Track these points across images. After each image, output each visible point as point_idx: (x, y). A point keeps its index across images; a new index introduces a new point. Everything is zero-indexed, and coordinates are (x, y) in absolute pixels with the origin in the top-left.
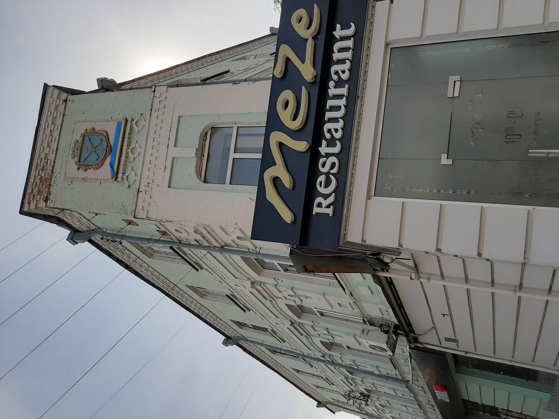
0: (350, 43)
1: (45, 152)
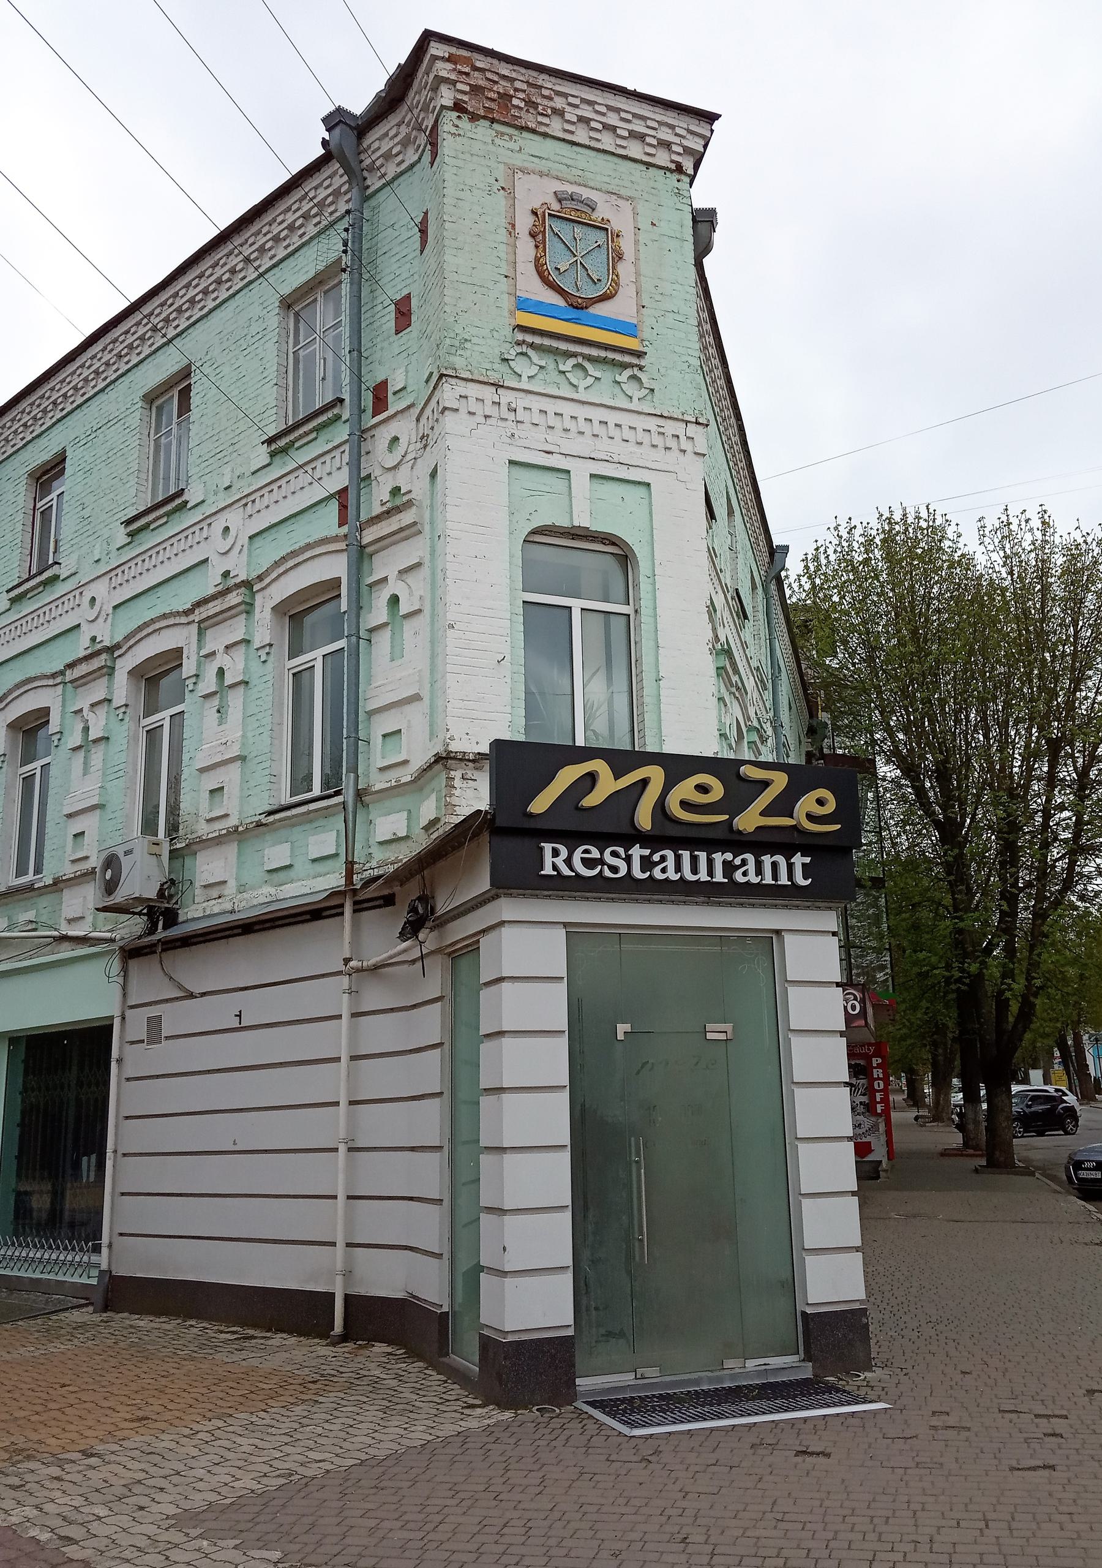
0: (784, 880)
1: (568, 109)
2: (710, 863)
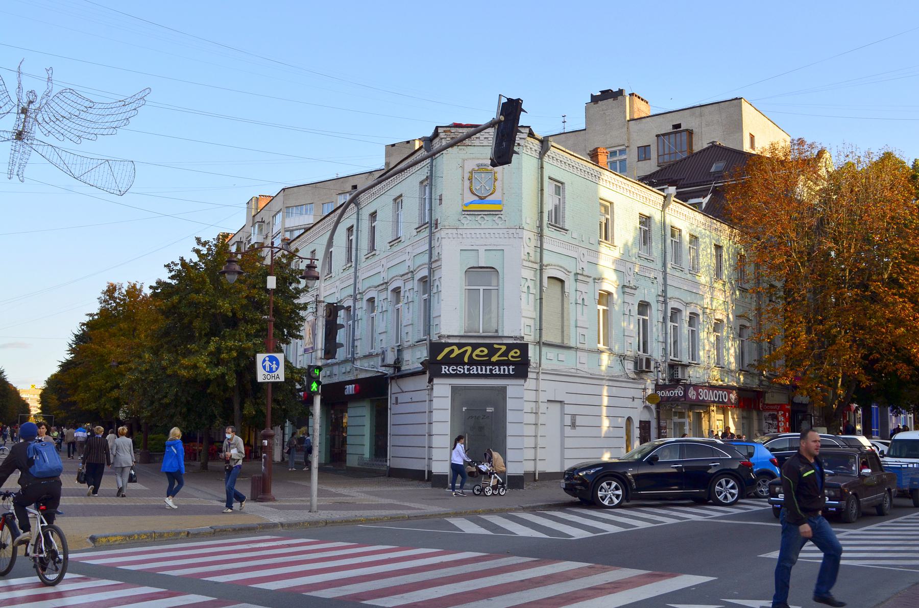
0: (506, 373)
1: (481, 136)
2: (486, 369)
